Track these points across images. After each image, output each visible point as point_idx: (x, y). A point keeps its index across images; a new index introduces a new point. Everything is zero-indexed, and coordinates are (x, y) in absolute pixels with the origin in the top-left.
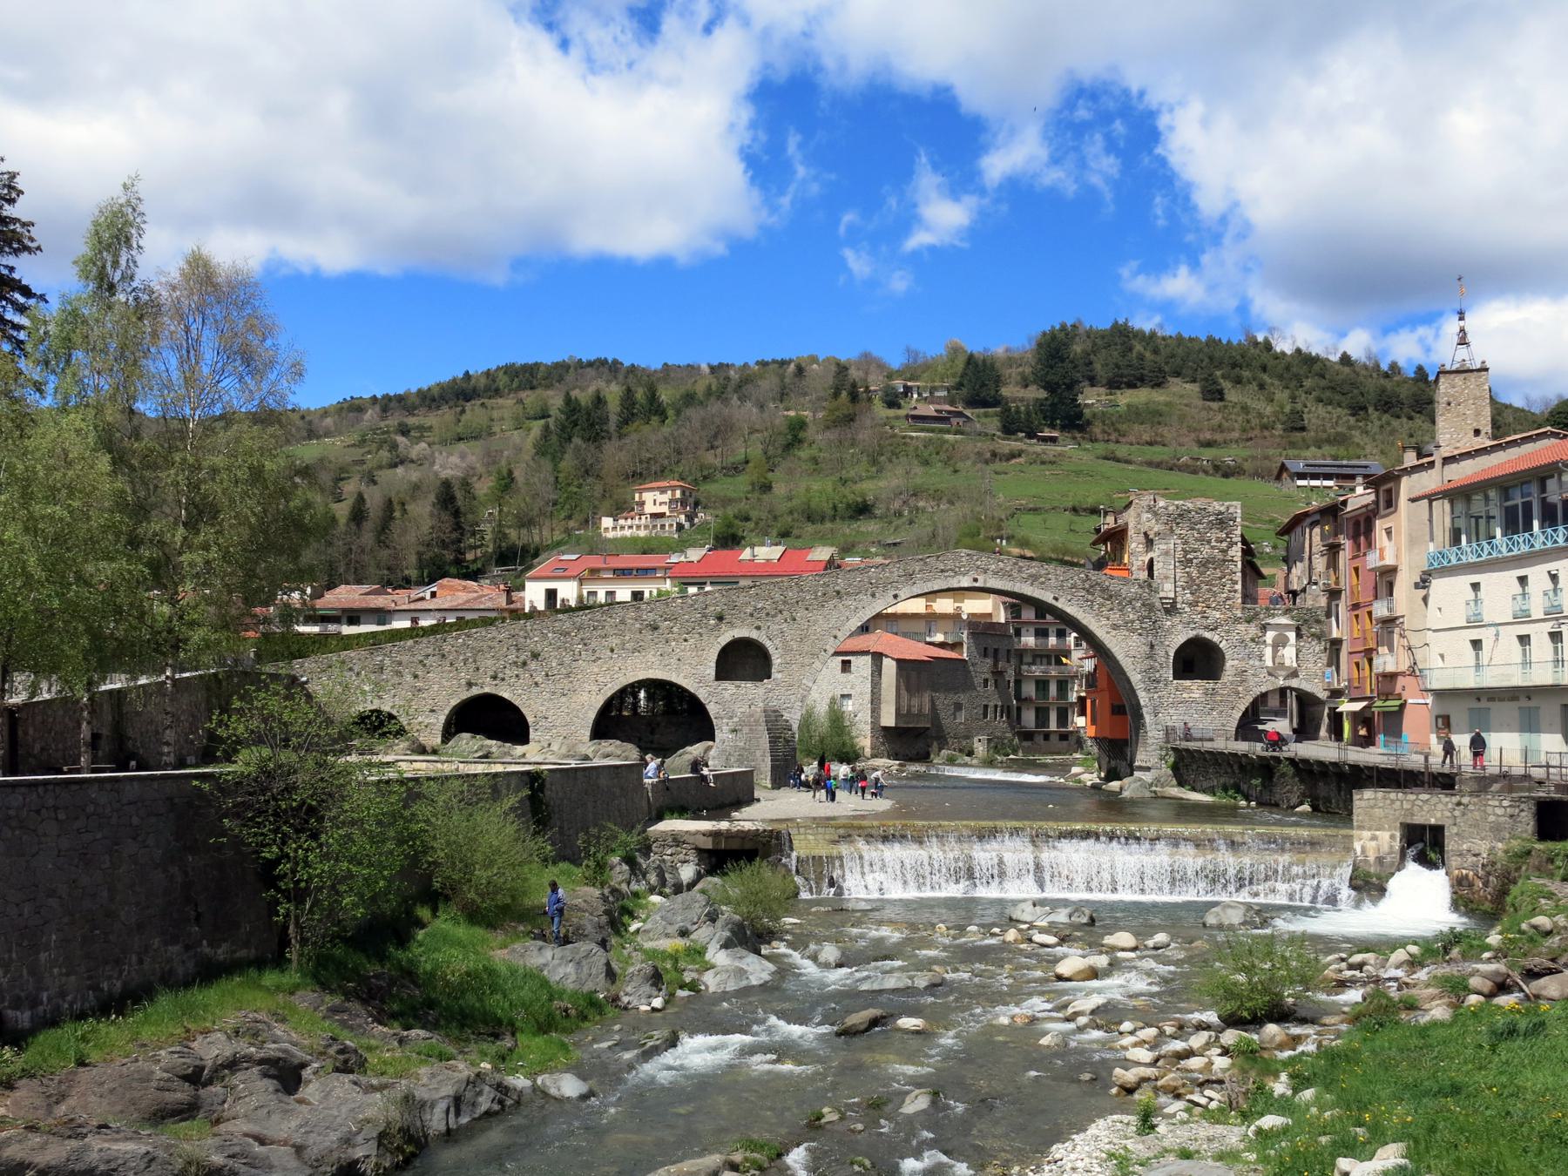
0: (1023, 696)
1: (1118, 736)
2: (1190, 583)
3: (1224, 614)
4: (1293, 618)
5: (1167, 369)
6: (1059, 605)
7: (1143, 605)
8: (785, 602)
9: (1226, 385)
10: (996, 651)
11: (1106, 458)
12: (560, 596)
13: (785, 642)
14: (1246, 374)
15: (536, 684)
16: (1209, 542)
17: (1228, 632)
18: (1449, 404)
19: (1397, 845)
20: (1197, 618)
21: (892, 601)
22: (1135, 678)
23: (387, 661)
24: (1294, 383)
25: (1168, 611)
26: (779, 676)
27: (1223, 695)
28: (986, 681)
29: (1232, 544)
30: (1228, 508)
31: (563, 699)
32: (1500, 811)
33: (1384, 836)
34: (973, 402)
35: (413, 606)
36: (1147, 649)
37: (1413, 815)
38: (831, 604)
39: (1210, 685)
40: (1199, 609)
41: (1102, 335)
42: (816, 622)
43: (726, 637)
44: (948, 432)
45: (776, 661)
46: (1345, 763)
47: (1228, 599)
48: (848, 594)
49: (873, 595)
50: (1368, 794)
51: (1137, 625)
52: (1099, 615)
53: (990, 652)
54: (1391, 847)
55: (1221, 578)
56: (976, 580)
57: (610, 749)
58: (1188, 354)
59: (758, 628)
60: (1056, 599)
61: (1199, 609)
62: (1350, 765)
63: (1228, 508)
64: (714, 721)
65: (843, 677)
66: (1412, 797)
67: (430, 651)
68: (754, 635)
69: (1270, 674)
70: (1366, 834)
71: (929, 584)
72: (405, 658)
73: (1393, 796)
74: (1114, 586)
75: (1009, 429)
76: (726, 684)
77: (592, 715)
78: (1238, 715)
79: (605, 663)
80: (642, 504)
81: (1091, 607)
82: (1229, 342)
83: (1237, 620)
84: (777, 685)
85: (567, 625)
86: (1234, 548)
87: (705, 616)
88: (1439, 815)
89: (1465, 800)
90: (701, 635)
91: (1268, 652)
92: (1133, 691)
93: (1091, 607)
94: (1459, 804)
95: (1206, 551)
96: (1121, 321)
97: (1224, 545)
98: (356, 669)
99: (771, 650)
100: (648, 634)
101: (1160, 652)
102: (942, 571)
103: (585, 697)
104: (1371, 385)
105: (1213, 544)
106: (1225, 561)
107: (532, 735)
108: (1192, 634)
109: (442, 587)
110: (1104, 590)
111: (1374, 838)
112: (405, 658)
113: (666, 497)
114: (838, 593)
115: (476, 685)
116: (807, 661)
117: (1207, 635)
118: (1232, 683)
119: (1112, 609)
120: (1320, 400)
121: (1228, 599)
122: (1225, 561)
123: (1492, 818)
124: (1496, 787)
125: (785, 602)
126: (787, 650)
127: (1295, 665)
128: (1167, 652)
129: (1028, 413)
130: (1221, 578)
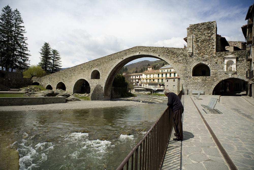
3: (210, 56)
7: (184, 55)
13: (102, 71)
16: (204, 34)
20: (200, 58)
25: (190, 56)
29: (212, 34)
39: (204, 77)
43: (92, 71)
45: (101, 75)
47: (211, 51)
48: (113, 59)
51: (182, 61)
52: (171, 59)
55: (208, 45)
60: (159, 56)
61: (201, 55)
65: (173, 82)
68: (97, 69)
69: (225, 73)
78: (213, 87)
83: (214, 57)
91: (225, 66)
95: (203, 37)
97: (210, 35)
102: (133, 52)
105: (206, 35)
108: (198, 63)
110: (172, 52)
114: (112, 59)
117: (204, 63)
119: (174, 57)
121: (211, 51)
126: (102, 72)
127: (235, 70)
130: (208, 45)
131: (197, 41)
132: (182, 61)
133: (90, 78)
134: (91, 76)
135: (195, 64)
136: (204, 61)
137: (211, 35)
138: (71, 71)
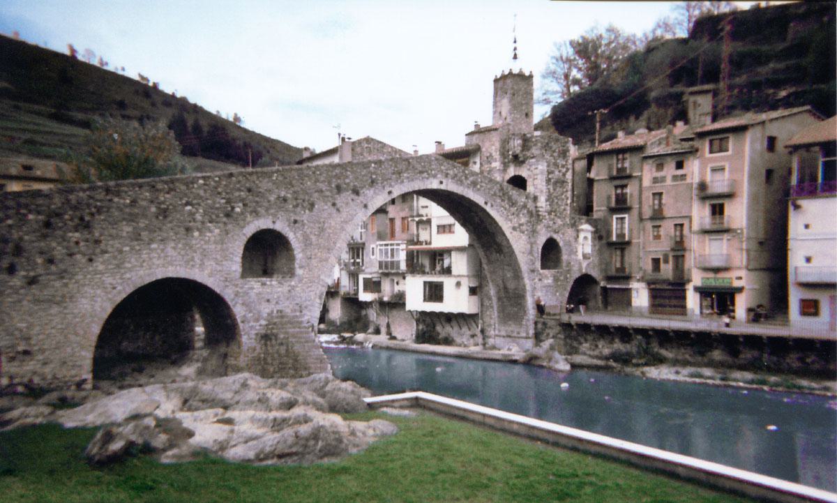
2: (550, 199)
6: (488, 208)
17: (563, 234)
20: (551, 223)
31: (55, 310)
36: (529, 246)
40: (552, 217)
43: (250, 230)
45: (299, 255)
52: (507, 219)
56: (441, 183)
60: (486, 203)
64: (241, 325)
77: (96, 329)
79: (115, 258)
84: (300, 281)
90: (225, 224)
101: (535, 249)
106: (564, 182)
108: (549, 236)
110: (510, 199)
117: (555, 236)
119: (513, 214)
121: (565, 210)
126: (307, 241)
128: (538, 249)
131: (548, 181)
132: (524, 228)
133: (238, 275)
134: (238, 259)
137: (567, 171)
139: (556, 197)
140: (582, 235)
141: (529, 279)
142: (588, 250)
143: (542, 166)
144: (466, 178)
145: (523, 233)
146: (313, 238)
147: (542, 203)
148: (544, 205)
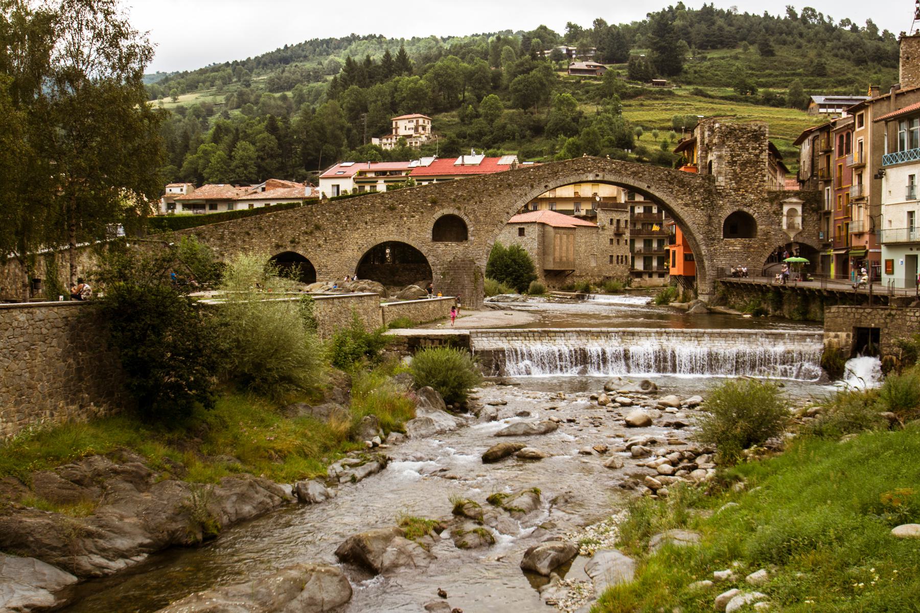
0: (636, 250)
1: (689, 274)
4: (800, 199)
5: (738, 36)
8: (476, 191)
9: (776, 47)
10: (618, 221)
11: (696, 94)
12: (341, 189)
13: (476, 217)
14: (790, 39)
15: (319, 246)
16: (748, 150)
17: (758, 207)
18: (908, 58)
19: (850, 341)
21: (543, 188)
22: (699, 237)
23: (226, 232)
24: (820, 43)
26: (472, 238)
27: (754, 248)
28: (611, 240)
29: (762, 151)
30: (760, 128)
31: (337, 255)
32: (914, 319)
33: (843, 335)
34: (610, 60)
35: (249, 197)
36: (706, 219)
37: (861, 322)
38: (505, 192)
39: (746, 241)
41: (697, 14)
42: (495, 204)
43: (438, 214)
44: (595, 79)
45: (471, 229)
46: (825, 290)
48: (516, 185)
49: (532, 186)
50: (834, 309)
51: (700, 203)
52: (676, 198)
53: (615, 222)
54: (847, 342)
57: (366, 286)
58: (752, 26)
59: (459, 209)
60: (649, 187)
62: (828, 292)
63: (760, 128)
66: (861, 311)
67: (252, 225)
68: (456, 213)
70: (832, 334)
71: (568, 179)
72: (237, 230)
73: (849, 310)
74: (687, 179)
75: (633, 77)
76: (439, 244)
77: (355, 264)
80: (397, 128)
81: (672, 192)
82: (779, 17)
85: (338, 207)
86: (764, 154)
87: (425, 201)
88: (877, 322)
89: (893, 312)
90: (422, 213)
92: (698, 246)
93: (672, 192)
94: (890, 315)
95: (745, 156)
96: (708, 5)
97: (757, 151)
98: (207, 237)
99: (467, 222)
100: (389, 214)
103: (349, 253)
104: (870, 44)
107: (318, 277)
108: (736, 209)
109: (268, 185)
111: (837, 336)
112: (237, 230)
113: (412, 125)
114: (509, 185)
115: (282, 246)
116: (490, 228)
117: (745, 209)
118: (761, 240)
120: (836, 55)
121: (759, 186)
122: (757, 162)
123: (908, 324)
124: (913, 304)
125: (476, 191)
126: (477, 221)
129: (646, 67)
131: (732, 163)
134: (430, 232)
135: (728, 212)
136: (745, 205)
138: (337, 213)
139: (746, 176)
140: (786, 209)
141: (707, 245)
142: (798, 220)
143: (725, 152)
144: (626, 170)
145: (698, 207)
146: (482, 219)
147: (721, 181)
148: (723, 184)
